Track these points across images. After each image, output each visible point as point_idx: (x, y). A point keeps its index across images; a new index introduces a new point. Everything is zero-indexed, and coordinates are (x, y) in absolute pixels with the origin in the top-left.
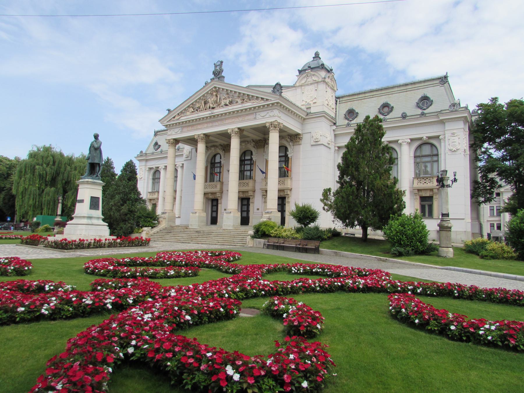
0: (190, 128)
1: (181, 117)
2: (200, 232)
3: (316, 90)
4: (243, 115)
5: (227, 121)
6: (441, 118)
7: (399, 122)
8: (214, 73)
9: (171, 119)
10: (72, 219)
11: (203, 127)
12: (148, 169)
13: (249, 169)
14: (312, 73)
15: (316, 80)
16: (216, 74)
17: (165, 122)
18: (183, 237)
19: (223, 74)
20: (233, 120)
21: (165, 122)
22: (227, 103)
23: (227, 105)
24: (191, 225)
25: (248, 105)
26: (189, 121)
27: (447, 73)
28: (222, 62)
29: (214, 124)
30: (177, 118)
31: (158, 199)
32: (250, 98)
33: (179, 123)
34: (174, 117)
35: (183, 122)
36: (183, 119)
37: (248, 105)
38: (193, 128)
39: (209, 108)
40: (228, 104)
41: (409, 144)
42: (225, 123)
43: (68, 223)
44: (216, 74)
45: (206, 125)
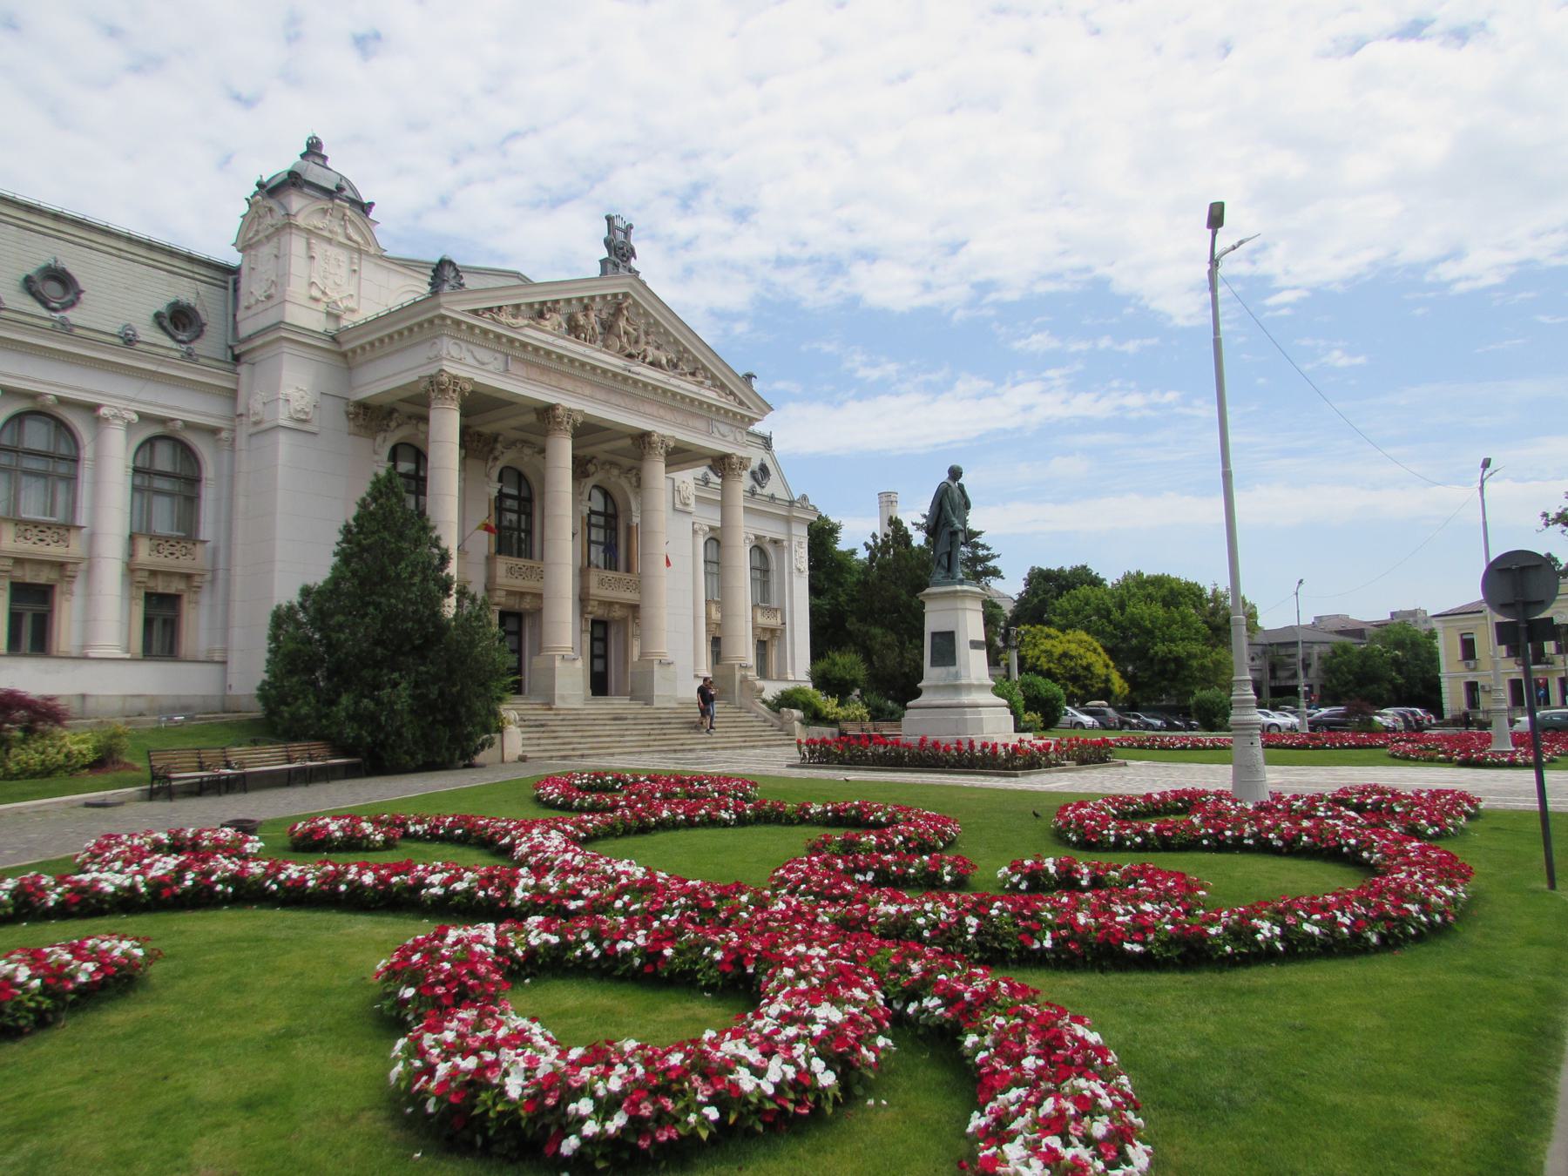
0: (535, 374)
1: (528, 326)
2: (626, 719)
4: (557, 372)
5: (648, 409)
10: (918, 693)
11: (579, 390)
16: (623, 255)
17: (459, 308)
18: (582, 737)
20: (662, 412)
21: (459, 308)
22: (664, 361)
23: (660, 366)
24: (563, 697)
25: (710, 395)
26: (583, 364)
28: (631, 227)
29: (614, 399)
30: (504, 318)
35: (524, 345)
36: (533, 335)
37: (710, 395)
38: (544, 378)
42: (579, 390)
43: (910, 704)
45: (588, 391)
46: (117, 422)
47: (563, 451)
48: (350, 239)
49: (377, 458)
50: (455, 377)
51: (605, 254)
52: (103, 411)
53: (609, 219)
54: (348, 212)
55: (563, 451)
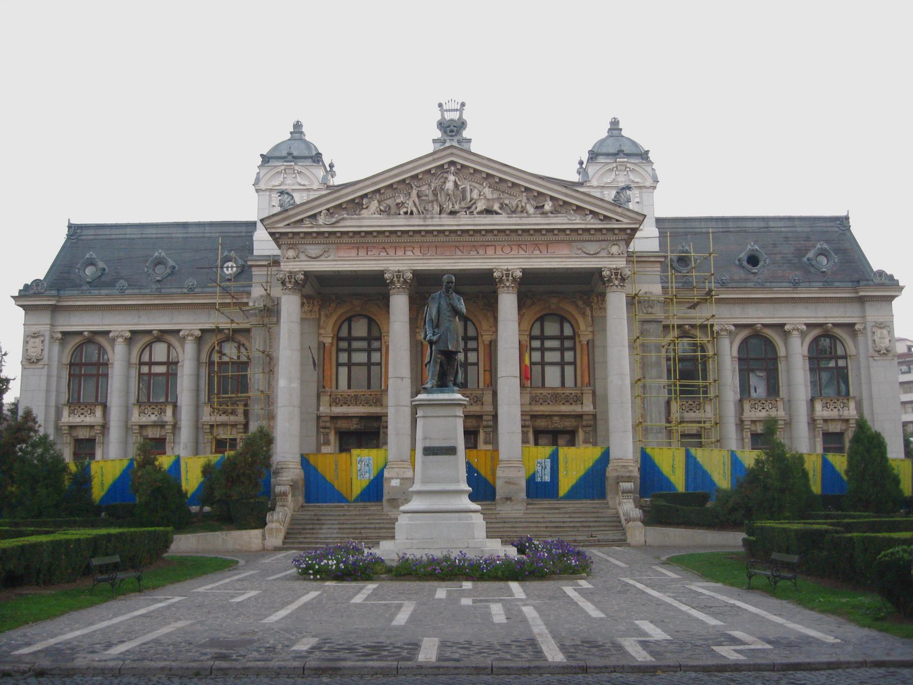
3: (638, 202)
6: (862, 294)
7: (816, 293)
8: (442, 125)
9: (302, 220)
12: (60, 336)
13: (540, 367)
14: (628, 165)
15: (638, 182)
16: (452, 131)
19: (466, 134)
22: (496, 207)
27: (848, 212)
28: (463, 105)
30: (321, 220)
31: (105, 427)
32: (561, 206)
33: (335, 233)
34: (314, 216)
36: (350, 224)
37: (561, 221)
39: (440, 213)
40: (499, 211)
41: (803, 334)
44: (452, 131)
46: (190, 338)
47: (400, 304)
48: (300, 184)
49: (322, 331)
50: (290, 272)
51: (438, 134)
52: (181, 333)
53: (440, 105)
54: (296, 168)
55: (400, 304)
